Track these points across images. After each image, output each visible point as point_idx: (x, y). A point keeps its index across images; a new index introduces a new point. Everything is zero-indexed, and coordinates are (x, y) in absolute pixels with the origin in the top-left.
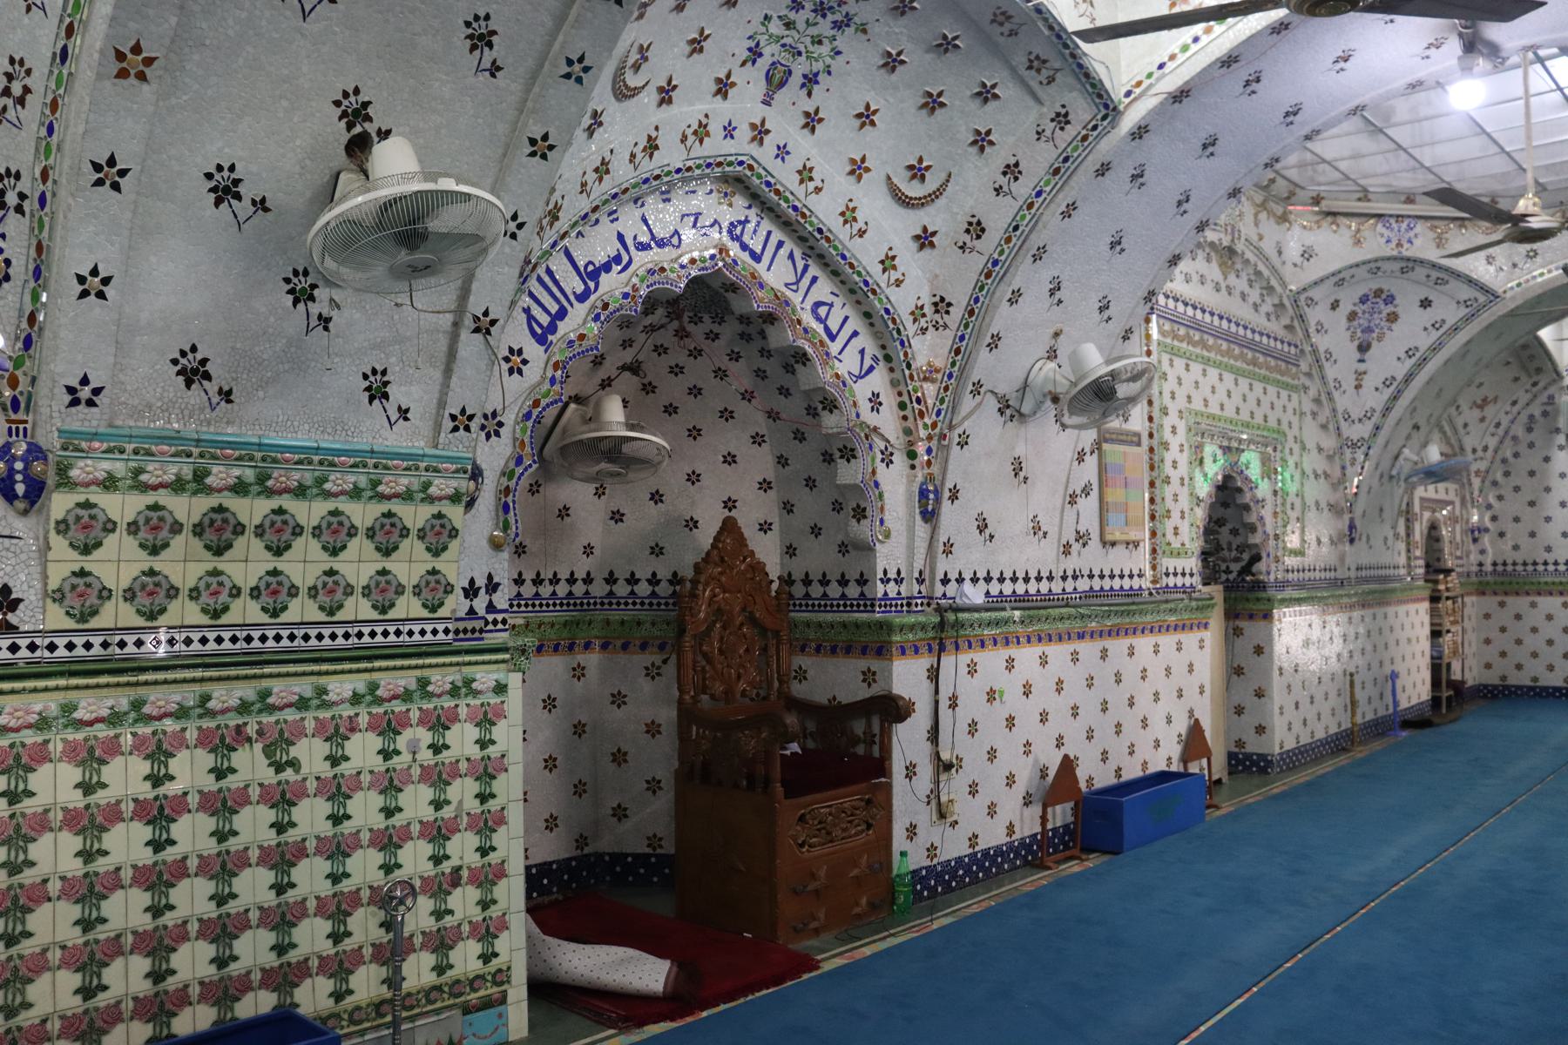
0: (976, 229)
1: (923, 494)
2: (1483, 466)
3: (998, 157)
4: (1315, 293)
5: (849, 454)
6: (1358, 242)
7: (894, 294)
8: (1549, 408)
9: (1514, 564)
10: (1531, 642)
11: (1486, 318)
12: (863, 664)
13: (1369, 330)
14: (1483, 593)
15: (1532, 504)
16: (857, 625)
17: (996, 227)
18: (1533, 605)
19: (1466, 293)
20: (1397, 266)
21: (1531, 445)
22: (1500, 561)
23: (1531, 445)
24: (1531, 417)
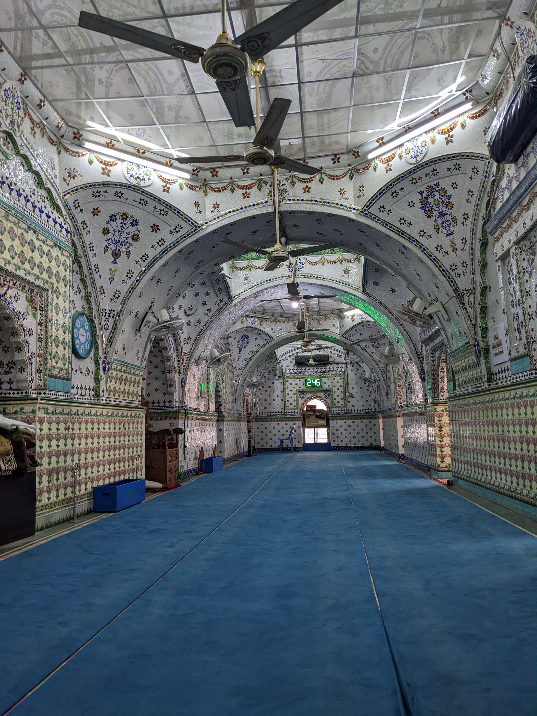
0: (199, 322)
1: (182, 382)
3: (207, 307)
4: (232, 335)
5: (170, 372)
6: (242, 323)
7: (181, 335)
10: (269, 435)
11: (271, 344)
12: (170, 421)
13: (242, 345)
15: (269, 396)
16: (169, 412)
17: (203, 322)
18: (270, 424)
19: (266, 337)
20: (251, 329)
21: (269, 379)
23: (269, 379)
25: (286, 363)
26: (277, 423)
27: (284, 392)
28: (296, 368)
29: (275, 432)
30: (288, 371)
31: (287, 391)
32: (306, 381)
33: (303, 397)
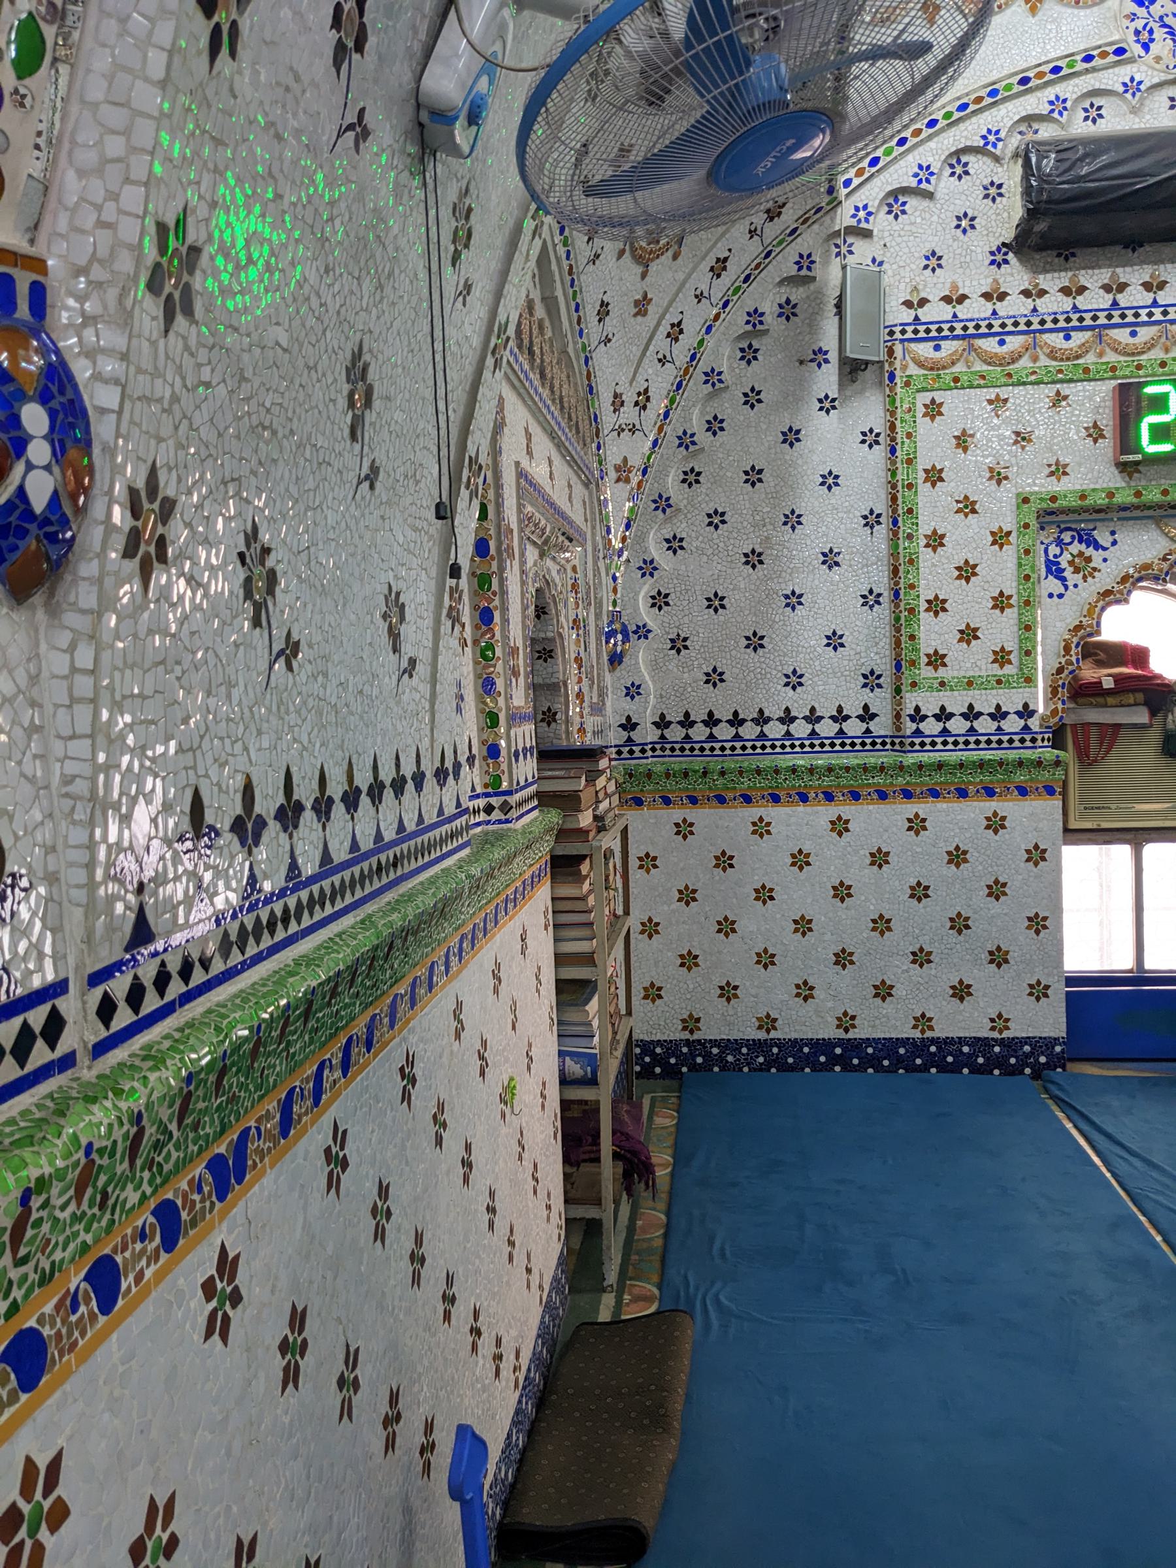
2: (636, 449)
8: (797, 294)
9: (711, 721)
14: (639, 802)
15: (753, 559)
18: (761, 828)
21: (752, 398)
22: (675, 716)
23: (752, 398)
24: (755, 315)
25: (925, 225)
26: (825, 813)
27: (893, 516)
28: (1015, 276)
29: (803, 894)
30: (937, 312)
31: (932, 508)
32: (1130, 402)
33: (1083, 566)
